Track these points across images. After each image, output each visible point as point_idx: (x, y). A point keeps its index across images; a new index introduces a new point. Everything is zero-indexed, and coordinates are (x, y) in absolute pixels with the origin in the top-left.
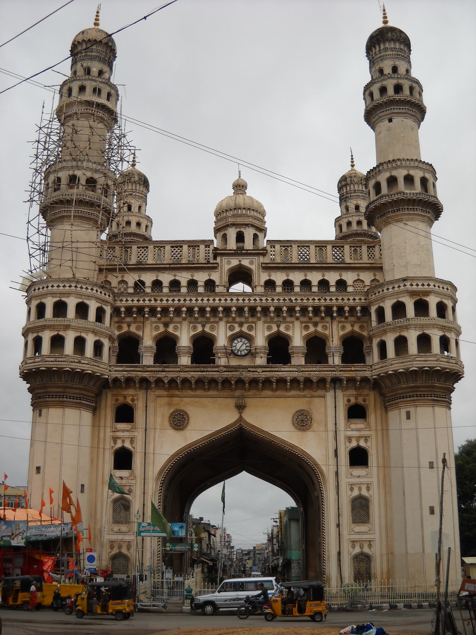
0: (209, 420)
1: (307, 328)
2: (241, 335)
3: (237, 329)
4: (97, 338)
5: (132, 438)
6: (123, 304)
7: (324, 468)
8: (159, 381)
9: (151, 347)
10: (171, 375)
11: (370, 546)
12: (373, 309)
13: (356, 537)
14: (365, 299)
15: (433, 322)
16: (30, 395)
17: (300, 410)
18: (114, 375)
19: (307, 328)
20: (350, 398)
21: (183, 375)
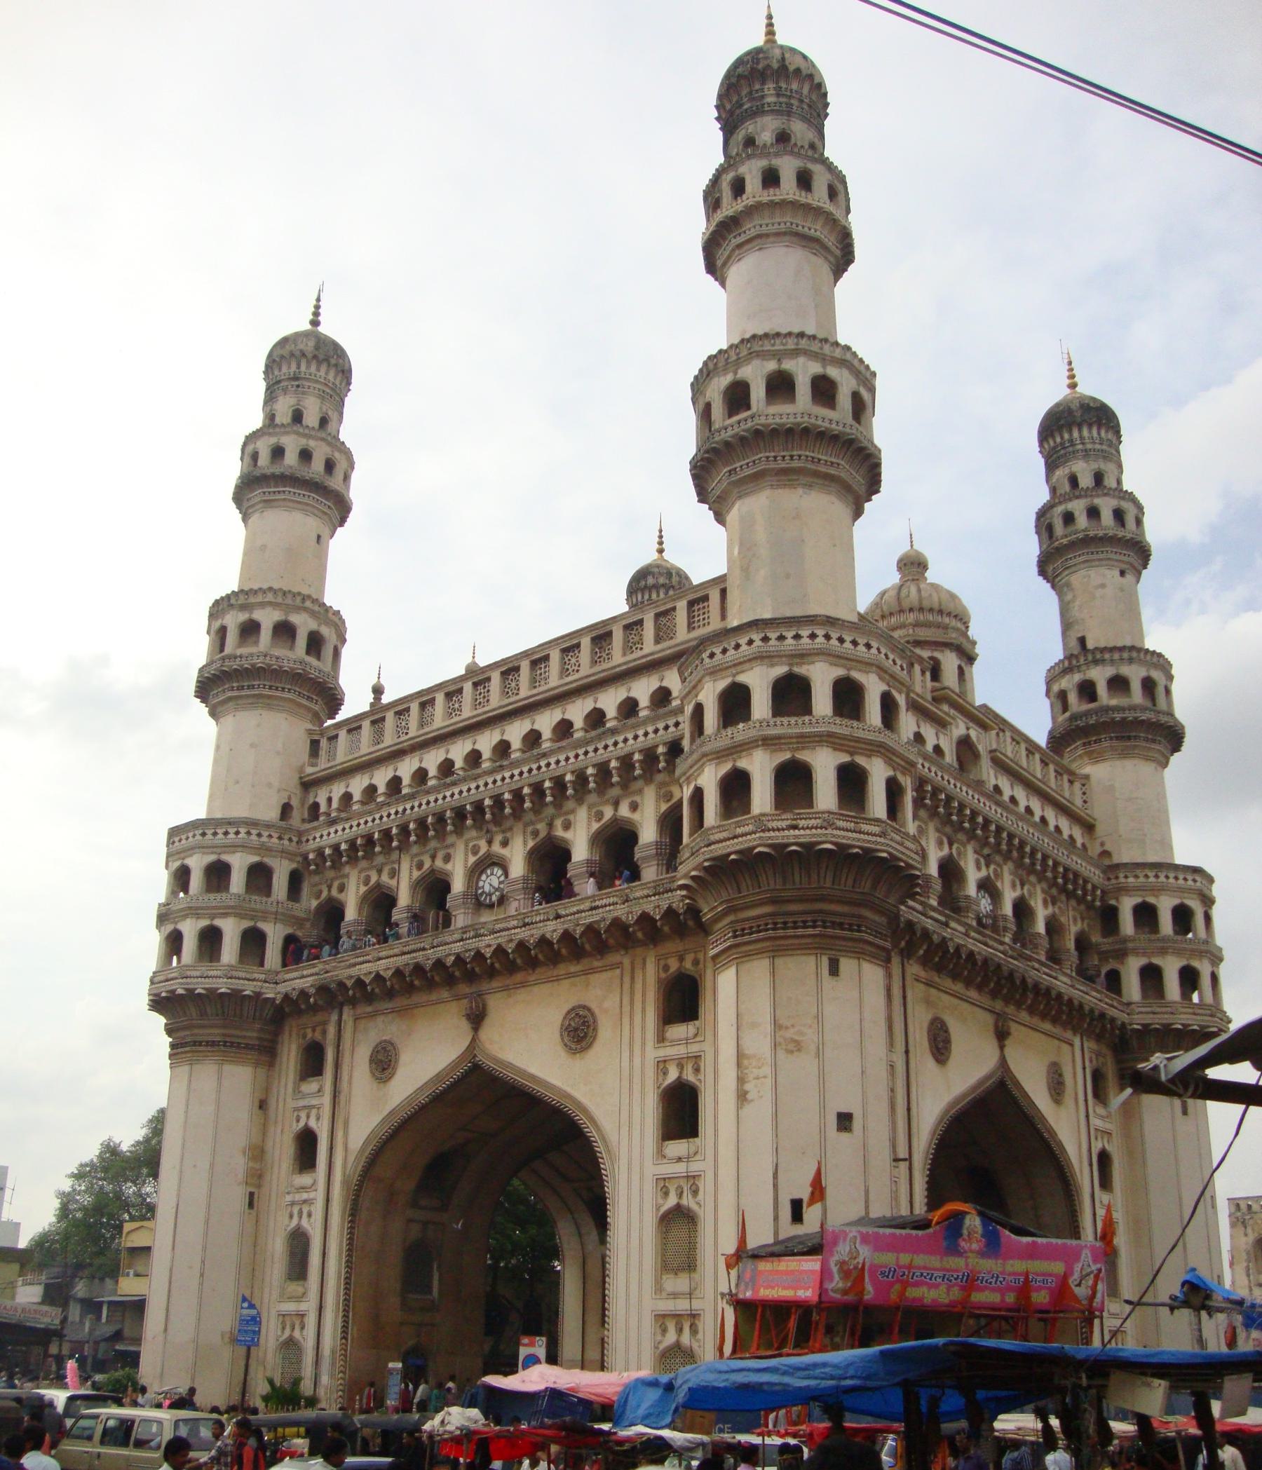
3: (484, 848)
4: (247, 924)
9: (356, 922)
10: (354, 971)
17: (573, 1009)
19: (599, 816)
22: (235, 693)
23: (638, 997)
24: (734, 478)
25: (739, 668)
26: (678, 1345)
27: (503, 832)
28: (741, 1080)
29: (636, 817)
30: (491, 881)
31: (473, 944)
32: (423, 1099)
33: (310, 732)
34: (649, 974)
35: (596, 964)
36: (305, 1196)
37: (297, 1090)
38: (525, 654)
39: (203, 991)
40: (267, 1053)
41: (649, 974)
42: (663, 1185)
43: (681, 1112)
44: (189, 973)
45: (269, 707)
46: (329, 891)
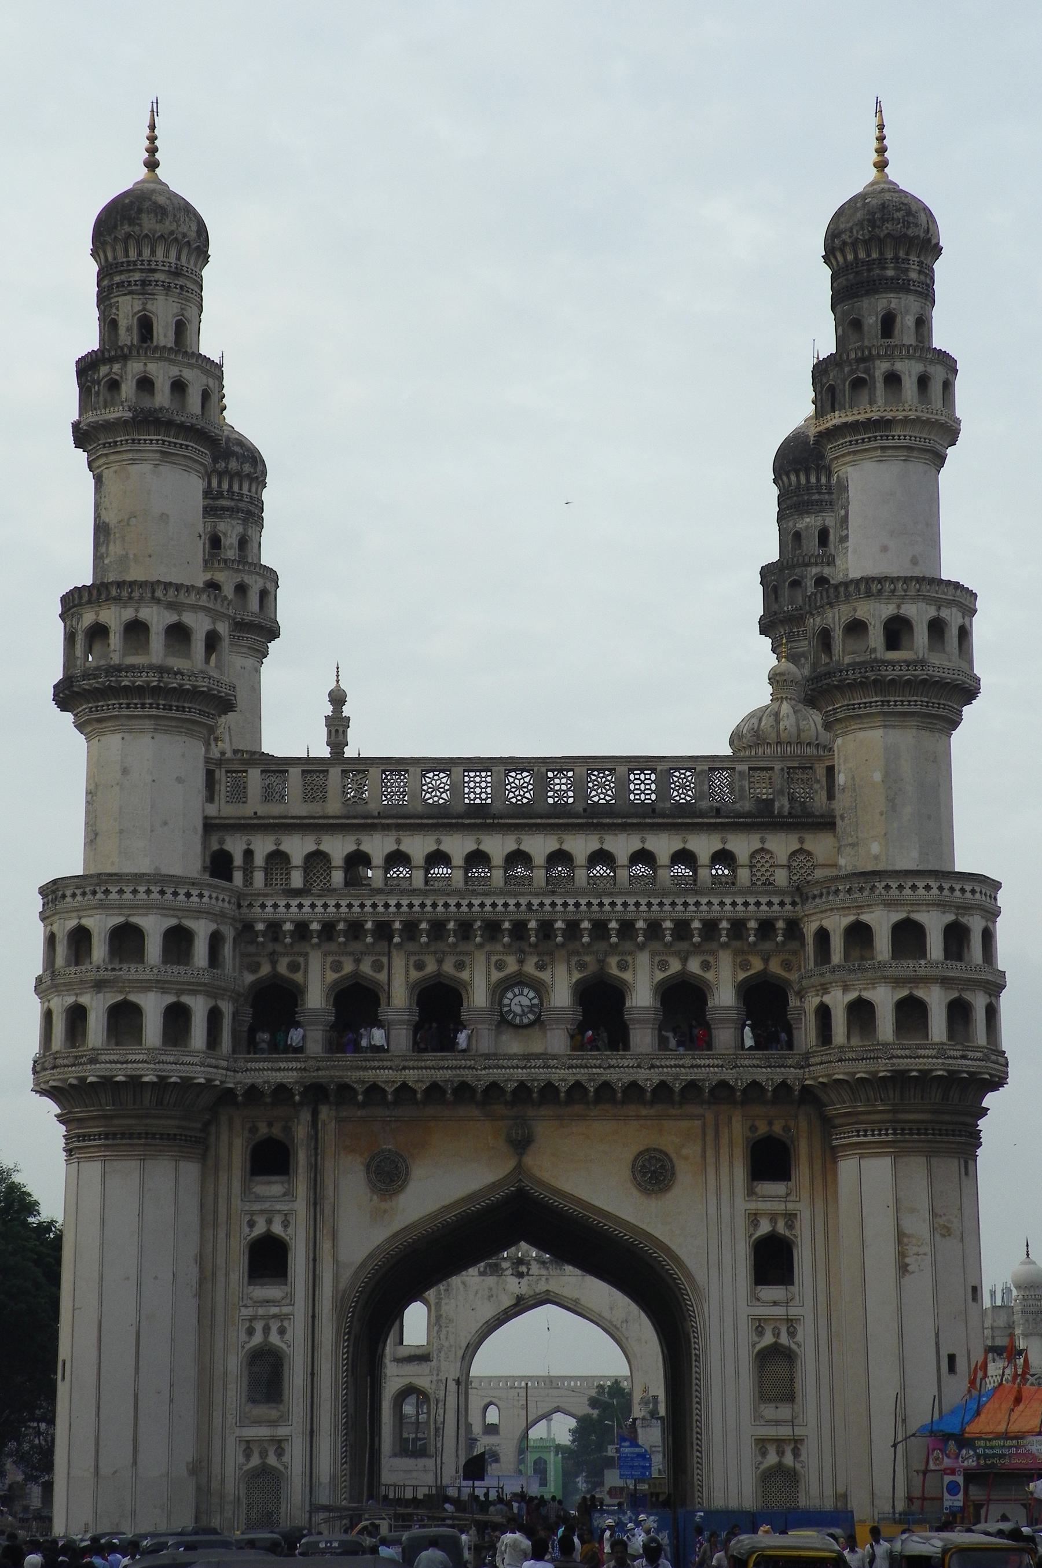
1: (663, 965)
2: (518, 981)
3: (512, 967)
4: (211, 1003)
5: (286, 1215)
6: (260, 916)
7: (700, 1277)
8: (345, 1091)
10: (369, 1076)
11: (796, 1453)
12: (810, 929)
13: (771, 1432)
14: (794, 904)
16: (62, 1129)
17: (647, 1150)
18: (248, 1079)
19: (663, 965)
20: (757, 1123)
21: (399, 1077)
22: (162, 713)
23: (724, 1151)
24: (886, 709)
25: (916, 908)
26: (780, 1465)
27: (539, 954)
28: (902, 1255)
29: (709, 976)
30: (519, 1001)
31: (543, 1074)
32: (449, 1217)
33: (208, 760)
35: (674, 1112)
36: (274, 1310)
37: (246, 1190)
39: (179, 1081)
43: (773, 1261)
44: (164, 1058)
46: (274, 968)
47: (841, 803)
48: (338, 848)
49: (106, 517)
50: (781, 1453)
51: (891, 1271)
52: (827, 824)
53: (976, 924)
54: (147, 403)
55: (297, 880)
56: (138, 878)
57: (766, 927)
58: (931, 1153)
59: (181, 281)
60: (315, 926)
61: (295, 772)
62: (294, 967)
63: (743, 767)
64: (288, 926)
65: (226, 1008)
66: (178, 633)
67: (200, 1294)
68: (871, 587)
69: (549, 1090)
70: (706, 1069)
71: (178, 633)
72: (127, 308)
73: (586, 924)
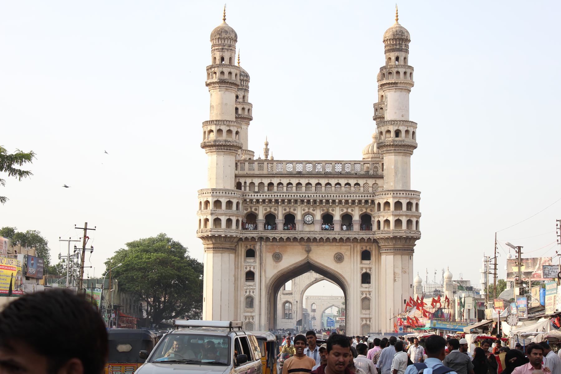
0: (292, 258)
1: (342, 210)
2: (308, 214)
3: (307, 210)
6: (248, 198)
8: (267, 239)
10: (273, 235)
11: (370, 321)
12: (376, 202)
13: (364, 316)
15: (404, 213)
19: (342, 210)
23: (355, 253)
28: (394, 277)
31: (314, 236)
32: (291, 267)
33: (236, 161)
34: (359, 249)
37: (245, 260)
38: (315, 161)
40: (234, 250)
41: (359, 249)
42: (362, 293)
43: (366, 278)
45: (232, 155)
47: (385, 173)
48: (266, 181)
49: (213, 104)
50: (366, 321)
51: (392, 281)
52: (382, 177)
53: (414, 202)
54: (222, 78)
55: (256, 189)
56: (220, 190)
57: (366, 202)
58: (402, 255)
59: (231, 48)
60: (261, 200)
61: (256, 163)
62: (256, 210)
63: (362, 163)
64: (254, 200)
65: (240, 219)
66: (229, 131)
67: (235, 284)
68: (393, 122)
69: (315, 239)
70: (352, 235)
71: (229, 131)
72: (218, 55)
73: (324, 201)
